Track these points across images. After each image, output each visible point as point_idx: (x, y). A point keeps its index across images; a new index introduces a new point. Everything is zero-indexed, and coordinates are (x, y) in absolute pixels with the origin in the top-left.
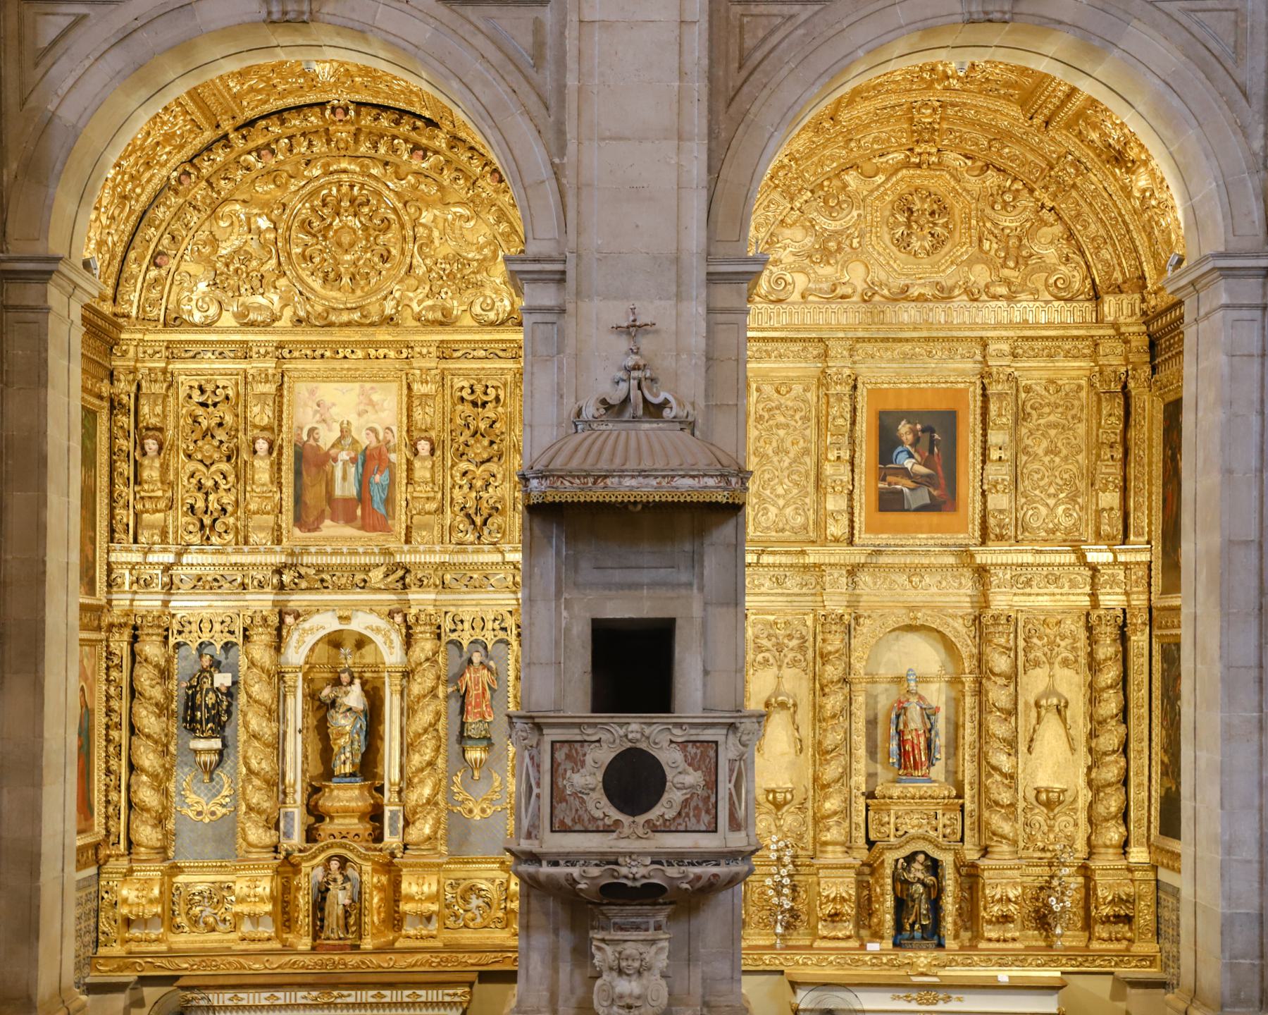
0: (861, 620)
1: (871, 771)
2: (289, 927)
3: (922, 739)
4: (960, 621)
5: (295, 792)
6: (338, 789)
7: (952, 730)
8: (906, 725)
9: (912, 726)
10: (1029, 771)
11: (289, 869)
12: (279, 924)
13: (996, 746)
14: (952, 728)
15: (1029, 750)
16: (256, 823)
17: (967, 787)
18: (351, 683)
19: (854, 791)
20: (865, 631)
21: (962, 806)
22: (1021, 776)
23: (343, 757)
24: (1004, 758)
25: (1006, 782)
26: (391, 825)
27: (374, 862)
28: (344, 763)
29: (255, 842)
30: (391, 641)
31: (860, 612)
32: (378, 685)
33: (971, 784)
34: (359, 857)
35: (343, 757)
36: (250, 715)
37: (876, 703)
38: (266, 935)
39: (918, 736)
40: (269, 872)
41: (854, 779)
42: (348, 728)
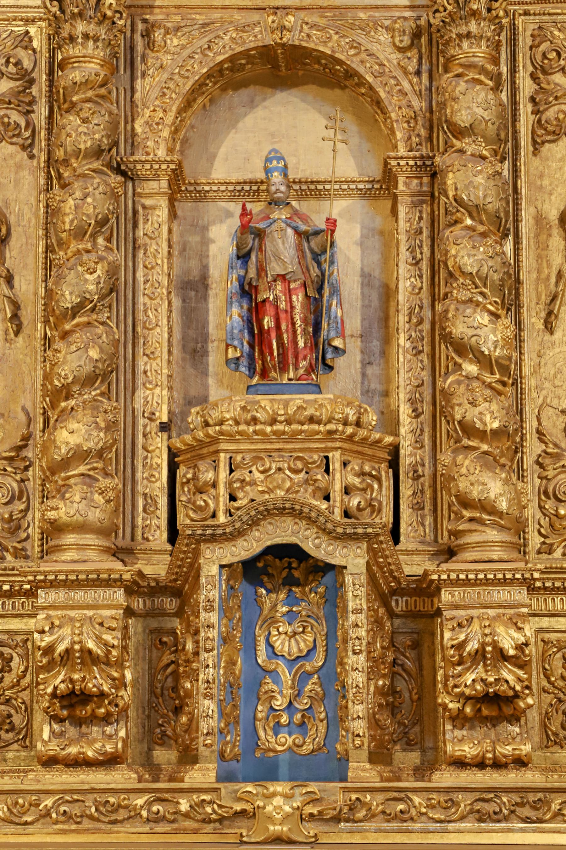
0: (158, 35)
1: (193, 392)
3: (298, 299)
4: (384, 37)
7: (376, 302)
8: (261, 270)
9: (274, 268)
10: (548, 371)
13: (464, 295)
14: (375, 296)
15: (549, 327)
17: (405, 411)
19: (141, 421)
20: (166, 59)
21: (395, 451)
22: (530, 383)
24: (484, 319)
25: (488, 378)
31: (156, 16)
33: (411, 401)
37: (206, 242)
39: (289, 293)
41: (140, 393)
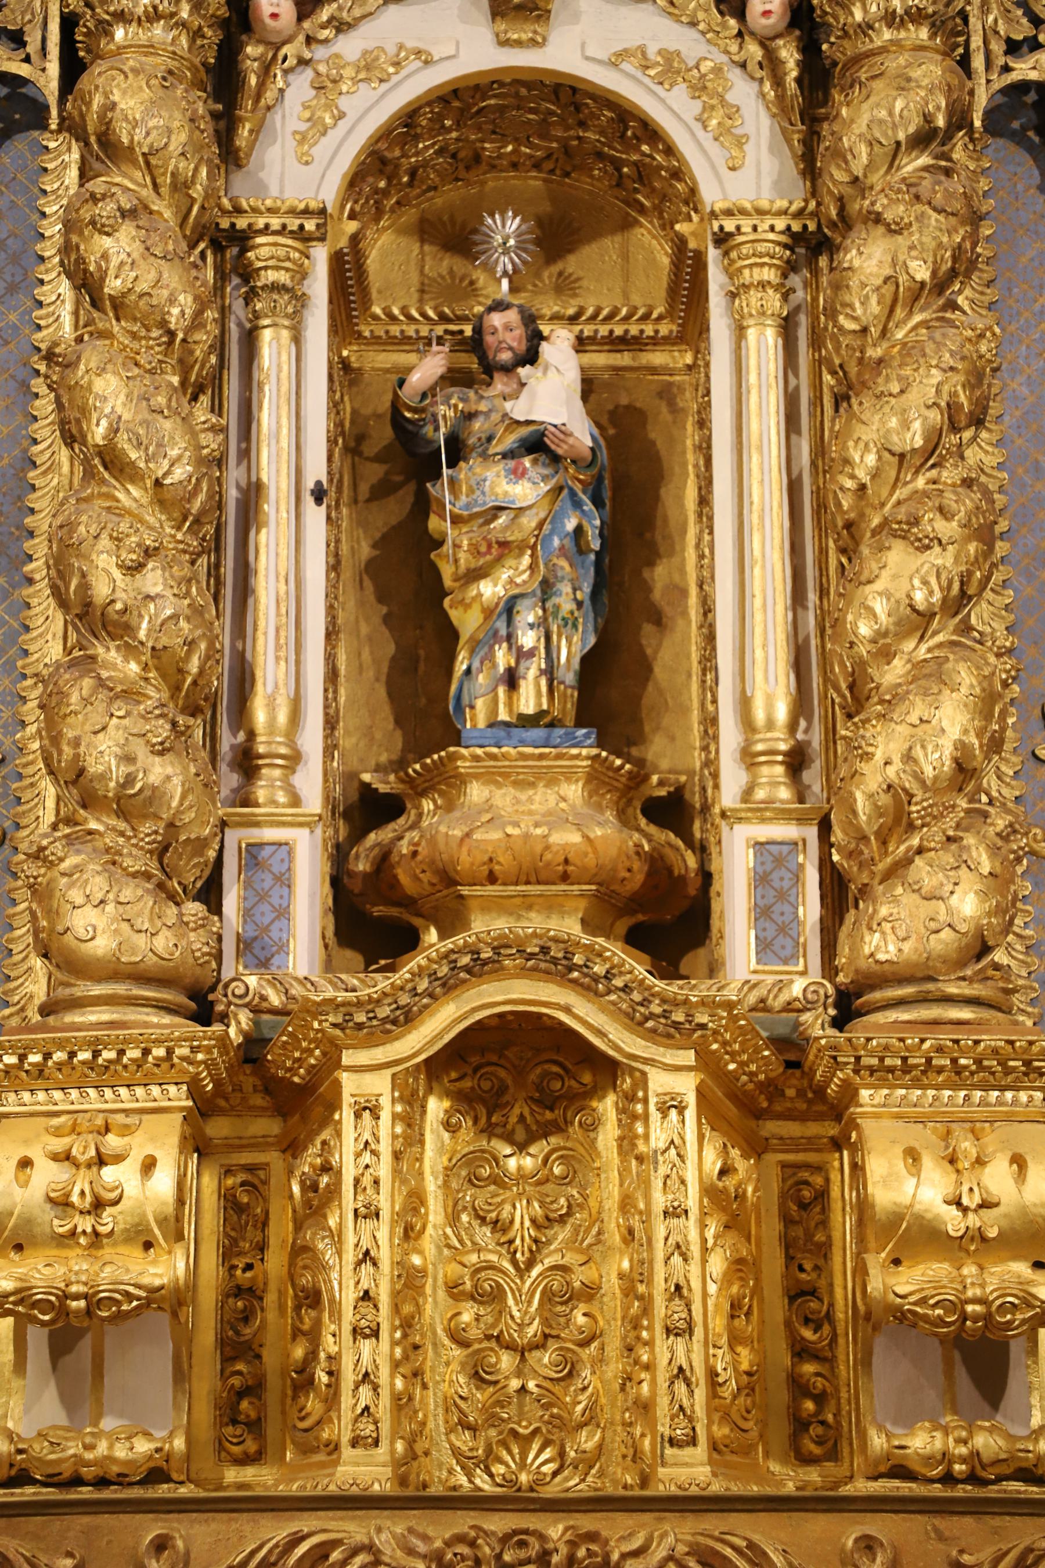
2: (255, 1426)
5: (294, 759)
6: (491, 777)
11: (269, 1126)
12: (204, 1413)
16: (112, 861)
18: (531, 357)
23: (502, 658)
26: (761, 913)
27: (707, 1062)
28: (511, 679)
29: (102, 946)
30: (733, 112)
32: (642, 399)
34: (636, 1022)
35: (502, 658)
36: (91, 357)
38: (143, 1446)
40: (178, 1096)
42: (529, 522)
